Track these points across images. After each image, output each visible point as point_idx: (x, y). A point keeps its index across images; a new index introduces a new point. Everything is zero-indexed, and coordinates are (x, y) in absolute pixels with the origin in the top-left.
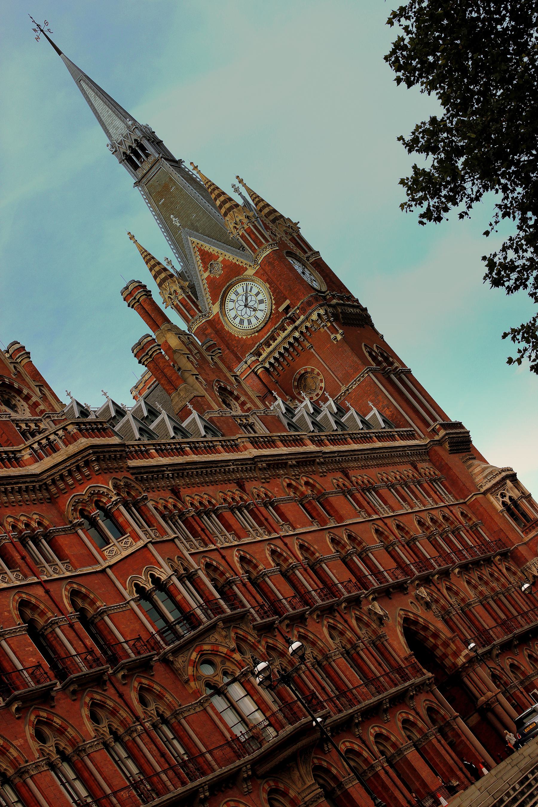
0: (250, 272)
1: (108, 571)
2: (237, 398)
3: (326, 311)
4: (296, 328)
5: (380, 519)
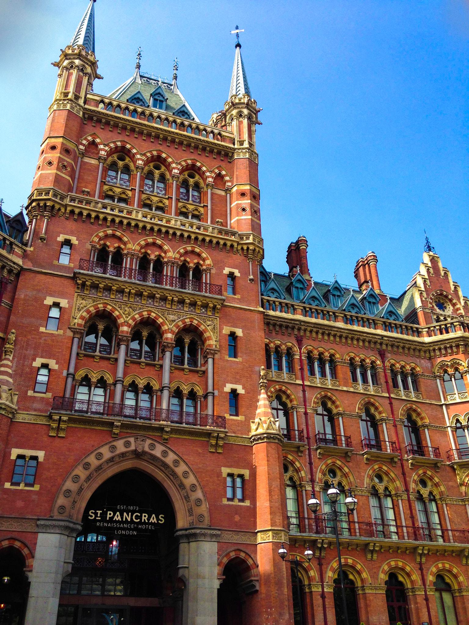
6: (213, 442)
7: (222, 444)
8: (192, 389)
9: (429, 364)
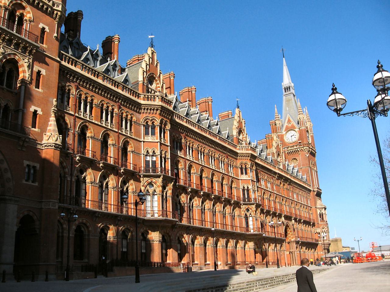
4: (299, 148)
6: (21, 143)
7: (26, 146)
8: (7, 104)
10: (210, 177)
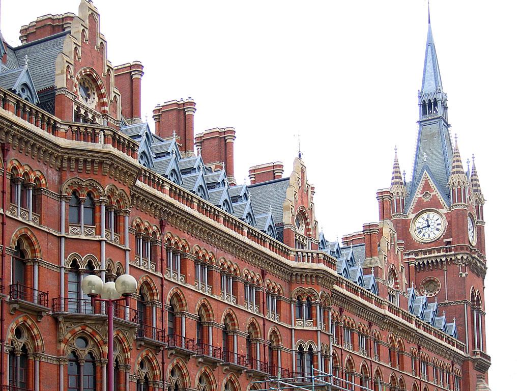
0: (444, 211)
1: (293, 330)
2: (396, 279)
3: (467, 258)
4: (445, 256)
5: (420, 380)
9: (57, 176)
10: (222, 322)
